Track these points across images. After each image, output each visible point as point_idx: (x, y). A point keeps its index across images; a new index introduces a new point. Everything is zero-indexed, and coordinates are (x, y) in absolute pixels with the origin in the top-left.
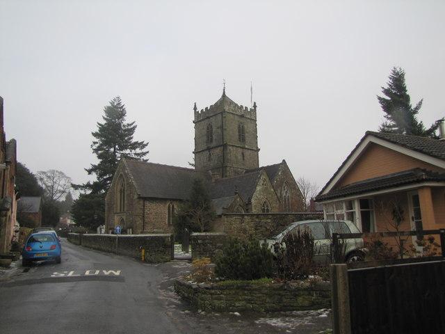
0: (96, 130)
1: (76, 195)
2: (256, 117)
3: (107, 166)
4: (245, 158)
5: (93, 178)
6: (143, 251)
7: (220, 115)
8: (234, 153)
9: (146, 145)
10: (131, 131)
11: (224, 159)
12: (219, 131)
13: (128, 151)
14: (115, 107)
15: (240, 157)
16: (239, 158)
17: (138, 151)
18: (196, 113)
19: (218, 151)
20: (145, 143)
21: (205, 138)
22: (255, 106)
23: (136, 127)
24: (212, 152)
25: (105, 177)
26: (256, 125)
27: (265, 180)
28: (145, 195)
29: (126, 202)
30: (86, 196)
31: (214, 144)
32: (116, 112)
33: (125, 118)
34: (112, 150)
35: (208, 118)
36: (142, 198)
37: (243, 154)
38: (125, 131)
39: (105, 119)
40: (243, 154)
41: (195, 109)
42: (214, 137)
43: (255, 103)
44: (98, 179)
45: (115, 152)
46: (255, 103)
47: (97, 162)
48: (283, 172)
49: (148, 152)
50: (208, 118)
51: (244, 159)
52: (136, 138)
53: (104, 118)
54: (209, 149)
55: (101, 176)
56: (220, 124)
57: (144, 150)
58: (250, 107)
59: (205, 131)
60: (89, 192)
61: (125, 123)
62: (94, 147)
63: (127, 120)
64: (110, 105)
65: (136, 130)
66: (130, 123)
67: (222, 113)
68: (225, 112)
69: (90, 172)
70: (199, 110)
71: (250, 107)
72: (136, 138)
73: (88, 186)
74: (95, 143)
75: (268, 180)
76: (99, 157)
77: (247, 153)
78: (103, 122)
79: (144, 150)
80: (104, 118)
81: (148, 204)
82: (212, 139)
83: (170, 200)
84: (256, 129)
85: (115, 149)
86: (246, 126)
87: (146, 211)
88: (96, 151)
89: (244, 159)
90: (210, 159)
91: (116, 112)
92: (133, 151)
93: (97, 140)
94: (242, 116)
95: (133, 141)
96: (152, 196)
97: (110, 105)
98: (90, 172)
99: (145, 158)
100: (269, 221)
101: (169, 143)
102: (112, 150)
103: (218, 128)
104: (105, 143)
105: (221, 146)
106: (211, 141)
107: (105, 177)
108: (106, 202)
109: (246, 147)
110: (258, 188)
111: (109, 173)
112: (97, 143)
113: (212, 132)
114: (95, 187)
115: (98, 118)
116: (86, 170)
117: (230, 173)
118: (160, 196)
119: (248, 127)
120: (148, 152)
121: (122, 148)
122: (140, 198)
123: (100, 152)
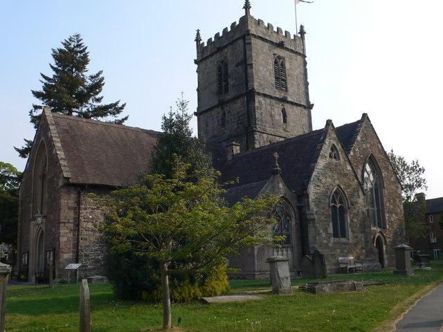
0: (40, 89)
2: (304, 50)
4: (288, 119)
7: (241, 42)
8: (264, 109)
10: (97, 86)
11: (249, 121)
12: (240, 69)
14: (71, 50)
16: (277, 117)
18: (200, 47)
19: (238, 106)
20: (120, 105)
21: (214, 87)
22: (302, 32)
23: (103, 79)
24: (227, 109)
26: (305, 63)
27: (333, 148)
28: (81, 180)
32: (70, 59)
33: (87, 66)
35: (220, 50)
36: (75, 186)
37: (284, 111)
40: (284, 111)
41: (198, 40)
42: (231, 82)
48: (365, 135)
50: (220, 50)
51: (285, 121)
54: (222, 104)
56: (241, 57)
57: (120, 117)
58: (293, 32)
59: (214, 77)
62: (35, 114)
63: (90, 70)
64: (63, 47)
66: (94, 73)
67: (243, 38)
68: (249, 34)
70: (204, 41)
71: (293, 32)
72: (107, 96)
74: (36, 107)
75: (339, 147)
77: (292, 112)
79: (120, 117)
82: (227, 85)
84: (305, 70)
86: (287, 65)
89: (285, 121)
91: (70, 59)
93: (39, 102)
94: (281, 45)
95: (104, 103)
97: (63, 47)
106: (227, 91)
109: (289, 99)
110: (321, 163)
112: (40, 107)
113: (226, 74)
116: (18, 150)
117: (261, 141)
119: (291, 65)
122: (69, 185)
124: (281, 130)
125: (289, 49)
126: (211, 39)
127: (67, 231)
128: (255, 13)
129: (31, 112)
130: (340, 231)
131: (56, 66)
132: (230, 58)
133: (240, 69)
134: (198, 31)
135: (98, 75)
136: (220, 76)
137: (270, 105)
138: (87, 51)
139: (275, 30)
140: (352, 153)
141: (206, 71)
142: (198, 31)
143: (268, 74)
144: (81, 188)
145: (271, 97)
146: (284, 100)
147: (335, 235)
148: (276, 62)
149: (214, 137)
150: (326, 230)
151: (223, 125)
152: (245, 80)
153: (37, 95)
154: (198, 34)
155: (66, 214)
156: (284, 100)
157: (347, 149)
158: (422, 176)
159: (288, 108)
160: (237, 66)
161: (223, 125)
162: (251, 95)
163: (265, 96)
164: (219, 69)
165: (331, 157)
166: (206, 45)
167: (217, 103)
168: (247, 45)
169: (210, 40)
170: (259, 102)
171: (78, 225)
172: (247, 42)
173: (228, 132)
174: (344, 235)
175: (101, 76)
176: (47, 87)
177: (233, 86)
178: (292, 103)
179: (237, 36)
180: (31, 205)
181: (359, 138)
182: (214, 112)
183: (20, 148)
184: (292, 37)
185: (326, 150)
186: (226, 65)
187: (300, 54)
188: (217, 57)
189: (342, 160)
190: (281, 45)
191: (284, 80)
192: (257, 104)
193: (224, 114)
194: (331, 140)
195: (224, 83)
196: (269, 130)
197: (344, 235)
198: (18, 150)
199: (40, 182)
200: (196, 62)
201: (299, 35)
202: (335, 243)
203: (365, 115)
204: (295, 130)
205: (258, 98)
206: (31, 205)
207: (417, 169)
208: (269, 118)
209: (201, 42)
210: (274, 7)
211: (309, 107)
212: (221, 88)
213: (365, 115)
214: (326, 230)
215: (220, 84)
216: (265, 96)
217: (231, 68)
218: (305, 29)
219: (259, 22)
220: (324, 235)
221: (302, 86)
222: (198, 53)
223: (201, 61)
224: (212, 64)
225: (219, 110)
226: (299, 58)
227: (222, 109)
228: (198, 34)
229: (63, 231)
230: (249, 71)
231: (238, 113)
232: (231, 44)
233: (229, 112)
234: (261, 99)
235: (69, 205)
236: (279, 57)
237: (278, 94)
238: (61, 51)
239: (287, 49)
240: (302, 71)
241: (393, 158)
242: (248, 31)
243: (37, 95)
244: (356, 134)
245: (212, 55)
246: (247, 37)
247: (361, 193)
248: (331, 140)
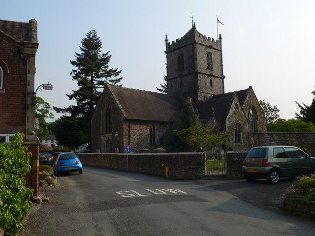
0: (75, 59)
1: (58, 116)
2: (221, 48)
3: (85, 92)
5: (74, 102)
6: (167, 168)
7: (191, 46)
8: (203, 80)
9: (120, 72)
10: (106, 60)
13: (103, 79)
15: (208, 84)
16: (208, 84)
17: (113, 78)
18: (167, 44)
20: (118, 71)
21: (176, 67)
22: (220, 38)
23: (111, 56)
25: (84, 102)
26: (222, 55)
27: (236, 104)
28: (130, 118)
29: (112, 124)
30: (66, 117)
31: (186, 72)
32: (91, 44)
33: (101, 49)
34: (90, 78)
36: (128, 120)
37: (211, 81)
38: (101, 60)
39: (83, 50)
40: (211, 81)
41: (166, 40)
42: (185, 66)
43: (220, 35)
44: (78, 104)
45: (92, 80)
46: (220, 35)
47: (77, 88)
49: (121, 78)
50: (179, 48)
51: (211, 86)
52: (111, 66)
53: (81, 48)
54: (180, 76)
55: (79, 101)
57: (118, 77)
58: (216, 38)
60: (69, 115)
61: (101, 53)
63: (103, 51)
64: (86, 37)
65: (111, 59)
66: (105, 52)
68: (195, 43)
69: (71, 97)
70: (170, 41)
71: (216, 38)
72: (111, 66)
73: (69, 110)
74: (74, 71)
75: (238, 104)
76: (79, 84)
79: (118, 77)
80: (81, 48)
81: (133, 126)
82: (183, 67)
83: (153, 121)
84: (222, 58)
85: (92, 77)
86: (213, 56)
88: (75, 78)
89: (211, 86)
90: (181, 85)
91: (91, 44)
92: (109, 79)
93: (76, 68)
94: (210, 47)
96: (136, 118)
97: (86, 37)
98: (71, 97)
99: (119, 84)
100: (294, 139)
101: (142, 70)
102: (90, 78)
103: (189, 58)
104: (83, 71)
106: (183, 70)
107: (84, 102)
108: (92, 124)
109: (214, 75)
110: (231, 111)
111: (87, 98)
112: (76, 71)
114: (74, 110)
115: (76, 48)
116: (68, 96)
117: (201, 98)
118: (144, 119)
120: (121, 78)
121: (98, 76)
122: (126, 120)
123: (80, 79)
124: (209, 90)
125: (214, 47)
128: (198, 29)
129: (71, 74)
130: (238, 140)
131: (83, 48)
134: (166, 35)
135: (107, 54)
138: (99, 40)
139: (207, 38)
140: (244, 105)
142: (166, 35)
144: (130, 121)
145: (205, 74)
146: (211, 75)
147: (236, 142)
149: (176, 92)
150: (232, 139)
153: (73, 63)
154: (166, 37)
155: (125, 132)
157: (242, 104)
158: (278, 113)
159: (213, 79)
160: (189, 58)
162: (196, 74)
163: (202, 74)
164: (179, 58)
166: (171, 44)
167: (178, 75)
168: (194, 48)
169: (173, 42)
170: (200, 77)
171: (129, 137)
174: (239, 142)
175: (109, 55)
176: (78, 59)
178: (215, 76)
179: (189, 43)
180: (101, 127)
181: (247, 98)
182: (175, 80)
183: (69, 94)
184: (215, 42)
185: (233, 105)
187: (219, 50)
189: (240, 110)
190: (210, 47)
191: (212, 65)
192: (199, 78)
193: (181, 81)
194: (235, 101)
196: (204, 91)
197: (239, 142)
198: (68, 96)
200: (165, 52)
201: (219, 40)
202: (236, 145)
203: (250, 87)
204: (216, 91)
205: (200, 75)
206: (101, 127)
207: (276, 110)
208: (204, 85)
209: (168, 42)
210: (207, 30)
211: (224, 77)
213: (250, 87)
214: (232, 139)
216: (202, 74)
218: (222, 37)
219: (200, 35)
220: (231, 142)
221: (220, 67)
225: (179, 79)
226: (219, 52)
227: (181, 79)
228: (166, 37)
230: (195, 61)
234: (201, 75)
236: (209, 53)
238: (85, 39)
239: (213, 48)
240: (220, 59)
241: (264, 104)
242: (195, 41)
243: (73, 63)
244: (246, 95)
245: (175, 50)
246: (194, 44)
247: (247, 123)
248: (235, 101)
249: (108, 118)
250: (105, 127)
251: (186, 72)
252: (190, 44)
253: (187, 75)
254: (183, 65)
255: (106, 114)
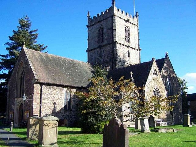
4: (130, 55)
7: (110, 18)
18: (89, 18)
19: (108, 48)
21: (97, 39)
24: (103, 49)
27: (155, 70)
29: (25, 87)
31: (105, 42)
35: (100, 21)
37: (128, 52)
40: (128, 52)
42: (105, 37)
51: (129, 56)
54: (100, 47)
56: (110, 26)
59: (96, 34)
68: (114, 16)
75: (157, 70)
78: (17, 30)
86: (130, 30)
87: (43, 96)
89: (129, 56)
93: (10, 41)
103: (108, 29)
105: (110, 44)
106: (103, 41)
126: (95, 16)
127: (36, 104)
132: (104, 26)
133: (110, 31)
136: (99, 34)
137: (123, 49)
141: (93, 31)
143: (122, 34)
144: (42, 84)
148: (126, 29)
151: (101, 57)
152: (112, 37)
155: (36, 96)
156: (128, 46)
159: (130, 50)
160: (108, 29)
161: (101, 57)
162: (114, 43)
164: (99, 31)
165: (154, 74)
166: (92, 19)
167: (97, 46)
168: (113, 21)
169: (94, 17)
172: (113, 19)
173: (102, 60)
177: (106, 39)
179: (109, 16)
180: (15, 91)
182: (95, 51)
185: (152, 71)
186: (103, 30)
188: (98, 25)
192: (117, 48)
193: (101, 52)
194: (155, 66)
195: (101, 38)
199: (19, 80)
200: (87, 26)
209: (90, 17)
212: (99, 40)
215: (99, 37)
217: (105, 30)
222: (88, 22)
223: (90, 26)
224: (96, 28)
229: (34, 104)
230: (114, 32)
231: (108, 52)
232: (105, 19)
233: (104, 51)
235: (37, 92)
237: (127, 44)
245: (95, 24)
246: (113, 17)
248: (155, 66)
249: (22, 81)
250: (19, 91)
251: (105, 42)
252: (110, 17)
253: (108, 44)
254: (102, 36)
255: (21, 77)
